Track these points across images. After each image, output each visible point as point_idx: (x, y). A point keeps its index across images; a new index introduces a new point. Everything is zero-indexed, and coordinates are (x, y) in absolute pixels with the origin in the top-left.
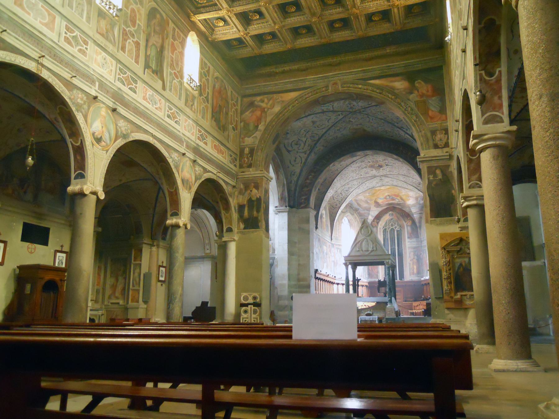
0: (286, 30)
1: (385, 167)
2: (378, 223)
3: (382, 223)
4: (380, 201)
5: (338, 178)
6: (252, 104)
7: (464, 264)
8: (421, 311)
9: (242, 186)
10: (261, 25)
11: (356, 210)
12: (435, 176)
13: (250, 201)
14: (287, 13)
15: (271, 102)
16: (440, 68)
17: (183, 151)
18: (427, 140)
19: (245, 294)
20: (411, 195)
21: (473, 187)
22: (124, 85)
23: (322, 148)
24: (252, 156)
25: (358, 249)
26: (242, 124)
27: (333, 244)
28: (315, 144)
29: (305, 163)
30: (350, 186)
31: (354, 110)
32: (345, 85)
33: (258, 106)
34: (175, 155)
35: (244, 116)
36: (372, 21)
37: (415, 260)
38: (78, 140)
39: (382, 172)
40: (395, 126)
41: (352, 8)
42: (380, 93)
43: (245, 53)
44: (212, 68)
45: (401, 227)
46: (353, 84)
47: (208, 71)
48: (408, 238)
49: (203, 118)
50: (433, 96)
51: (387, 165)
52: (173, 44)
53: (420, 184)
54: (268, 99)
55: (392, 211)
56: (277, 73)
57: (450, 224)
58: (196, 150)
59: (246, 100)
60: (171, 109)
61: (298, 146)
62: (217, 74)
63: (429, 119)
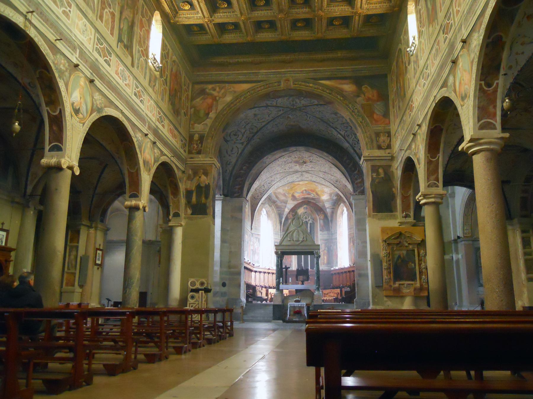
0: (250, 22)
1: (308, 164)
4: (297, 195)
5: (265, 170)
6: (203, 92)
7: (402, 256)
8: (332, 298)
9: (190, 172)
10: (227, 14)
11: (274, 202)
12: (378, 174)
13: (199, 187)
14: (256, 6)
15: (223, 91)
16: (385, 76)
17: (146, 132)
18: (372, 141)
19: (192, 280)
21: (432, 187)
22: (100, 56)
23: (258, 140)
24: (201, 143)
25: (289, 239)
26: (193, 110)
28: (253, 136)
29: (241, 153)
30: (272, 179)
31: (295, 107)
32: (297, 83)
33: (208, 94)
34: (139, 135)
35: (194, 102)
36: (333, 25)
37: (326, 251)
38: (56, 109)
39: (304, 168)
40: (330, 126)
41: (318, 10)
42: (330, 94)
43: (203, 40)
44: (171, 50)
45: (314, 220)
46: (304, 82)
47: (168, 53)
49: (162, 100)
50: (378, 101)
51: (311, 162)
52: (141, 20)
53: (337, 181)
54: (219, 88)
56: (230, 64)
57: (390, 219)
58: (156, 132)
59: (197, 87)
60: (137, 87)
61: (236, 137)
62: (174, 58)
63: (374, 122)
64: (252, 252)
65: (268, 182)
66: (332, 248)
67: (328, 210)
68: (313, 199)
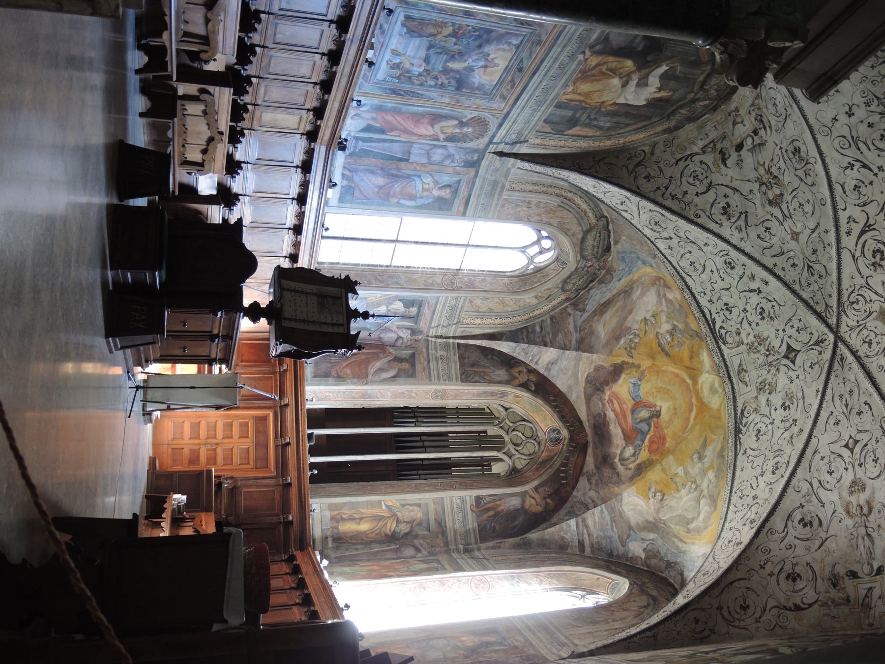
2: (524, 386)
3: (522, 402)
4: (623, 387)
11: (576, 302)
20: (671, 502)
27: (474, 164)
30: (759, 210)
45: (514, 476)
48: (478, 499)
53: (804, 523)
55: (571, 439)
64: (397, 150)
65: (735, 200)
66: (409, 552)
67: (572, 522)
68: (605, 460)
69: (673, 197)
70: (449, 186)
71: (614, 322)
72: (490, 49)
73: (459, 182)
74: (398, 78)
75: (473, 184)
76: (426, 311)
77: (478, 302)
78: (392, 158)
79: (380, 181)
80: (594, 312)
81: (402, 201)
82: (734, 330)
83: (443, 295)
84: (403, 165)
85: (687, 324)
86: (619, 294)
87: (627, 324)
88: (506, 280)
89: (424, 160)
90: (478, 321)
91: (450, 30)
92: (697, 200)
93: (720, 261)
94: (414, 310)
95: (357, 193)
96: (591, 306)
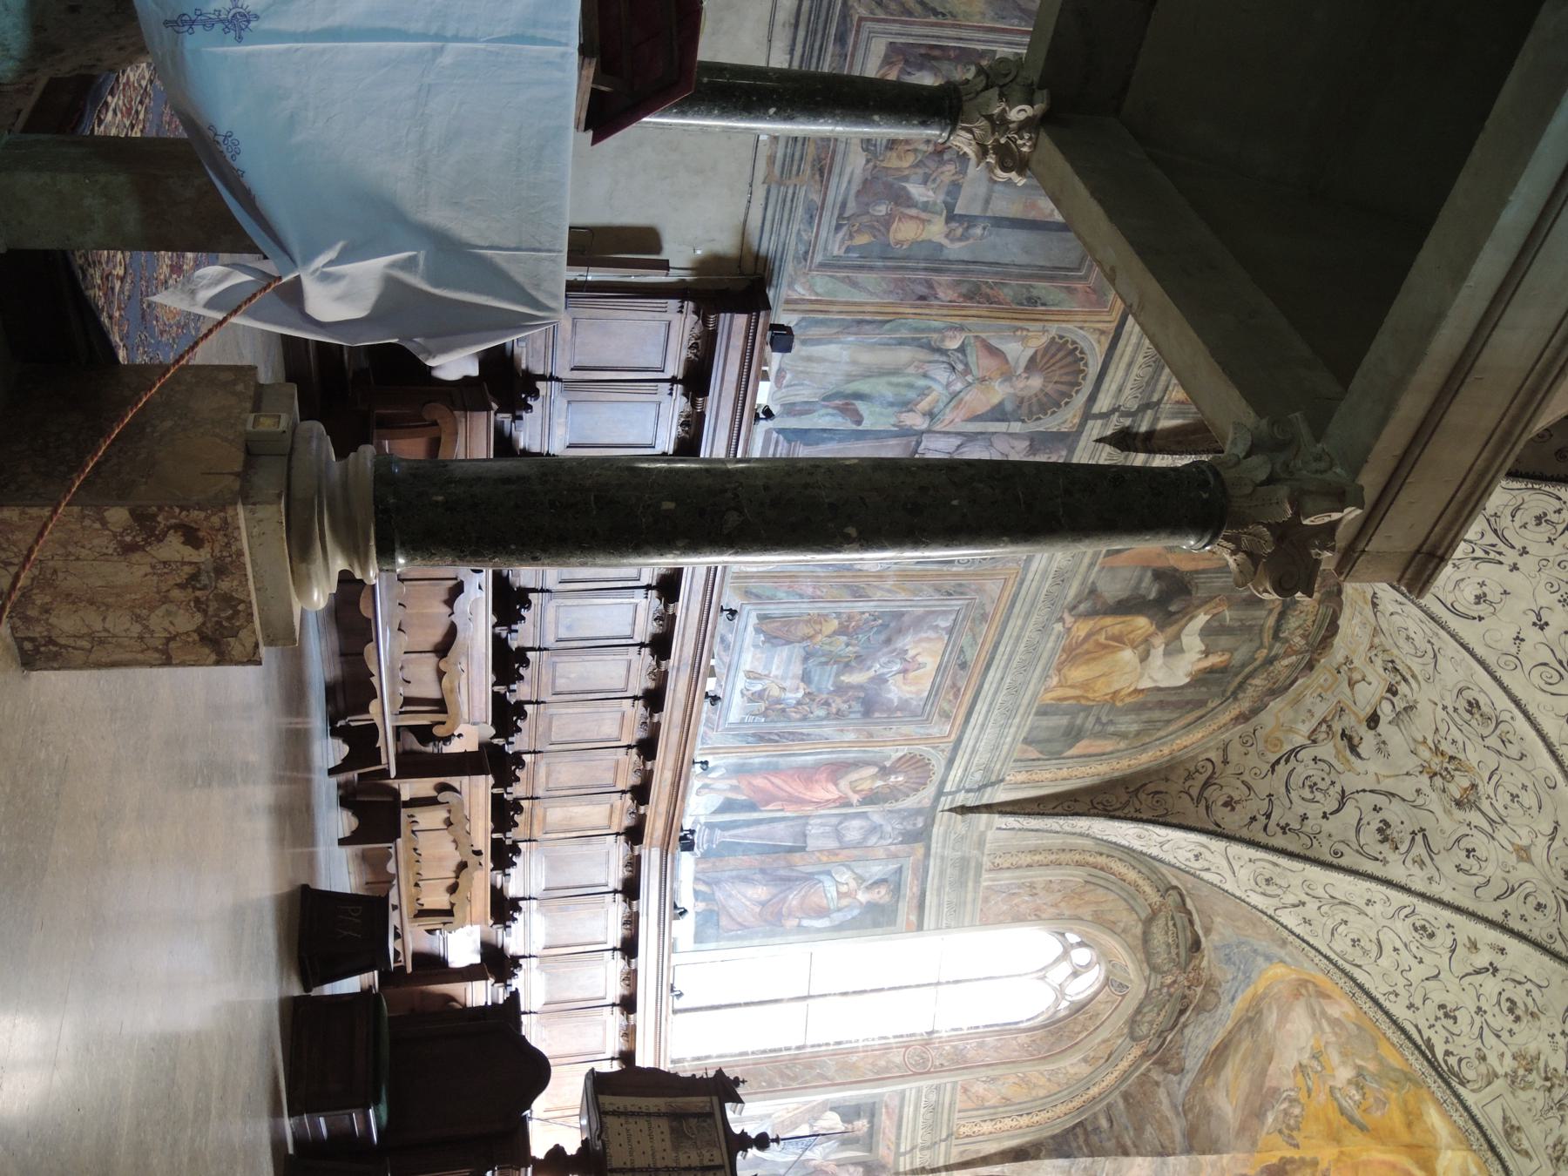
11: (1163, 1057)
27: (920, 836)
30: (1445, 822)
64: (782, 834)
65: (1394, 812)
69: (1284, 829)
70: (883, 881)
71: (1244, 1082)
72: (907, 642)
73: (900, 869)
74: (764, 714)
75: (926, 871)
76: (885, 1122)
77: (979, 1088)
78: (775, 849)
79: (761, 892)
80: (1201, 1070)
81: (805, 923)
82: (1470, 1052)
83: (910, 1087)
84: (797, 857)
85: (1381, 1061)
86: (1238, 1027)
87: (1270, 1083)
88: (1023, 1038)
89: (832, 844)
90: (987, 1127)
91: (835, 624)
92: (1327, 826)
93: (1403, 927)
94: (862, 1125)
95: (724, 921)
96: (1193, 1062)
